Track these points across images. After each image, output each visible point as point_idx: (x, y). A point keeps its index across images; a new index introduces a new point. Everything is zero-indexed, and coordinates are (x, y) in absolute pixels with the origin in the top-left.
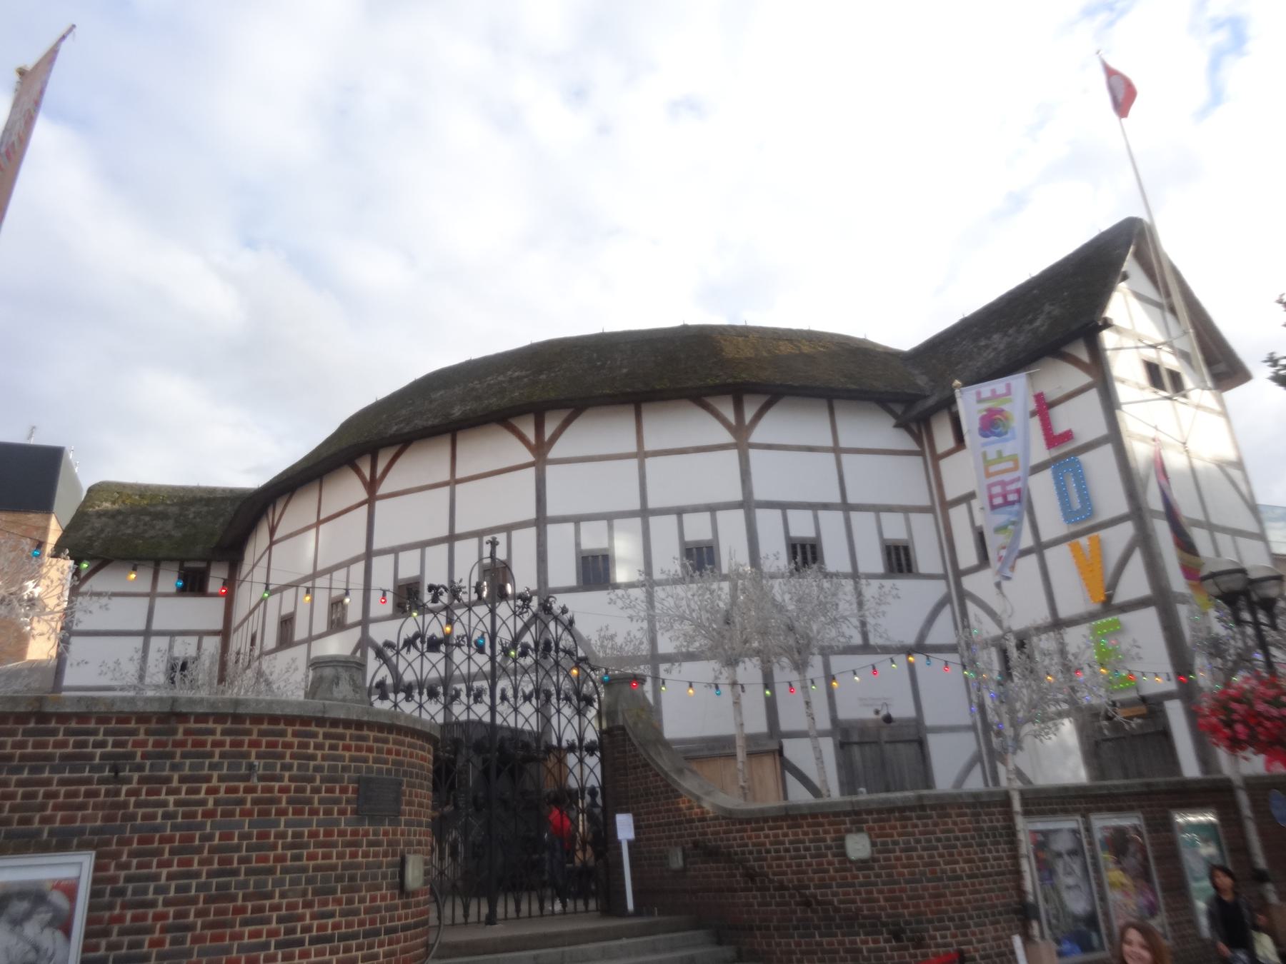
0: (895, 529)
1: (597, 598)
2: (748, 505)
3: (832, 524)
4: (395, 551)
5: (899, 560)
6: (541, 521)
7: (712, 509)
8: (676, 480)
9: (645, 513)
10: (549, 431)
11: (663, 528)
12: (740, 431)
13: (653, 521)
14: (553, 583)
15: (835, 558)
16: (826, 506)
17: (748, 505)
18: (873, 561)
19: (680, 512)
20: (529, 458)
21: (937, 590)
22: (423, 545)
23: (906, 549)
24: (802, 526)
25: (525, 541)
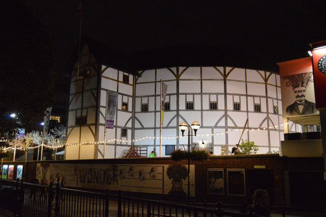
0: (257, 101)
1: (190, 112)
2: (225, 94)
3: (243, 99)
4: (141, 97)
5: (257, 109)
6: (178, 94)
7: (217, 94)
8: (208, 87)
9: (201, 94)
10: (180, 73)
11: (206, 98)
12: (225, 76)
13: (204, 96)
14: (180, 109)
15: (243, 107)
16: (242, 95)
17: (225, 94)
18: (251, 108)
19: (210, 94)
20: (175, 78)
21: (265, 115)
22: (148, 96)
23: (259, 106)
24: (237, 100)
25: (174, 98)
